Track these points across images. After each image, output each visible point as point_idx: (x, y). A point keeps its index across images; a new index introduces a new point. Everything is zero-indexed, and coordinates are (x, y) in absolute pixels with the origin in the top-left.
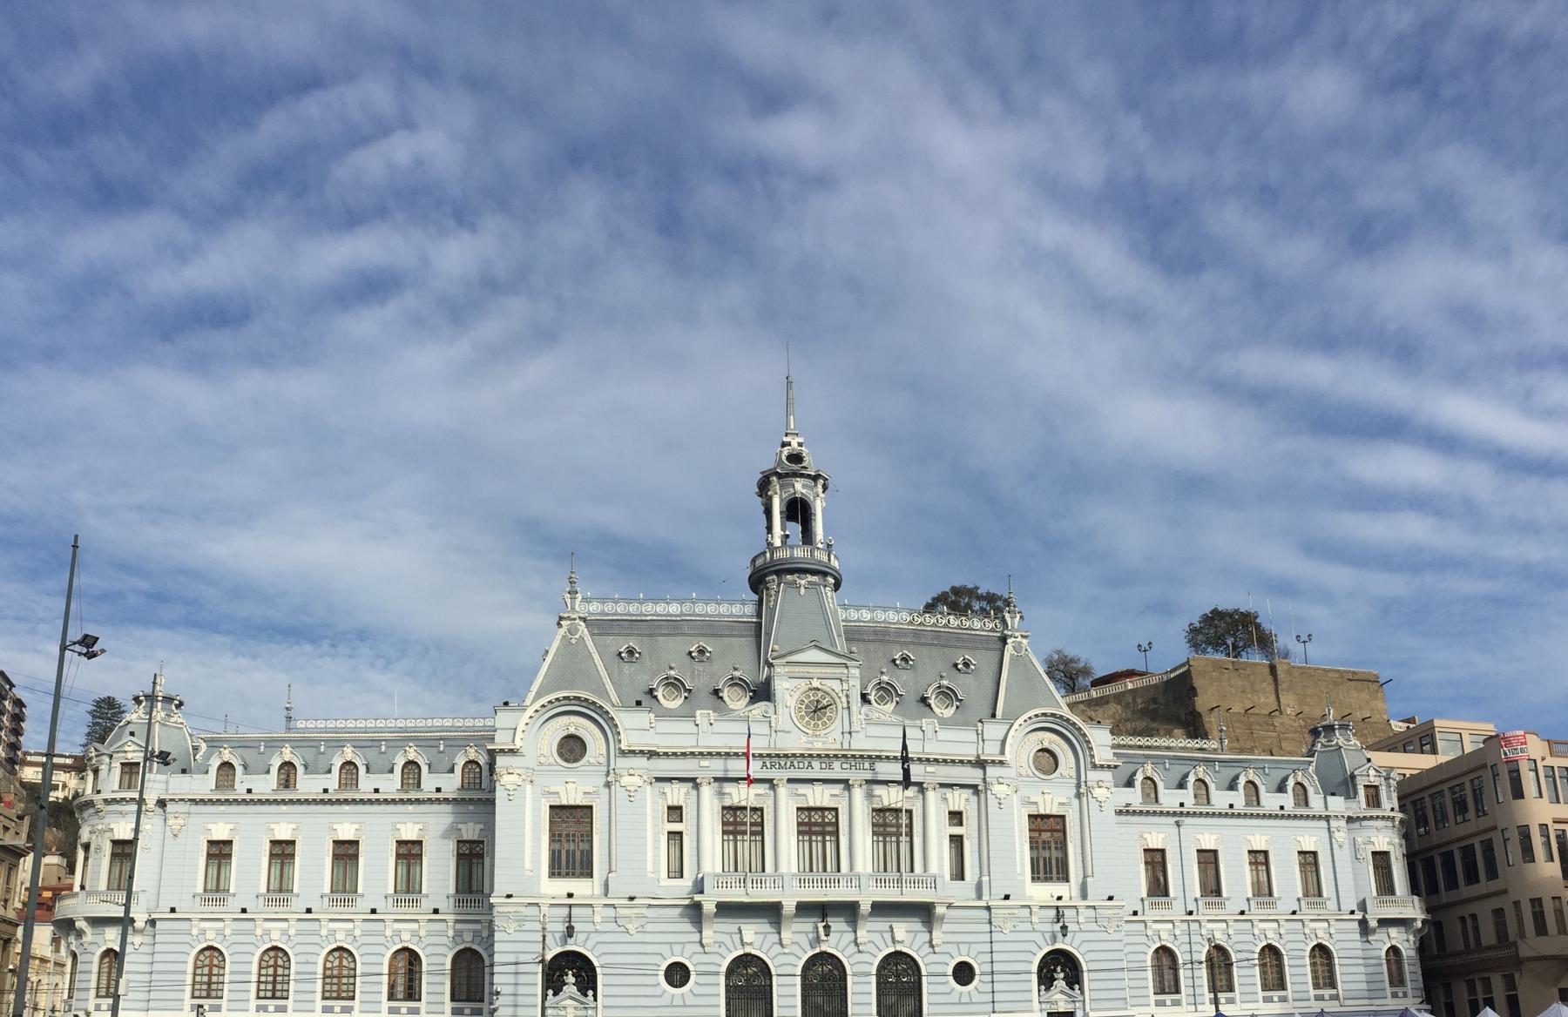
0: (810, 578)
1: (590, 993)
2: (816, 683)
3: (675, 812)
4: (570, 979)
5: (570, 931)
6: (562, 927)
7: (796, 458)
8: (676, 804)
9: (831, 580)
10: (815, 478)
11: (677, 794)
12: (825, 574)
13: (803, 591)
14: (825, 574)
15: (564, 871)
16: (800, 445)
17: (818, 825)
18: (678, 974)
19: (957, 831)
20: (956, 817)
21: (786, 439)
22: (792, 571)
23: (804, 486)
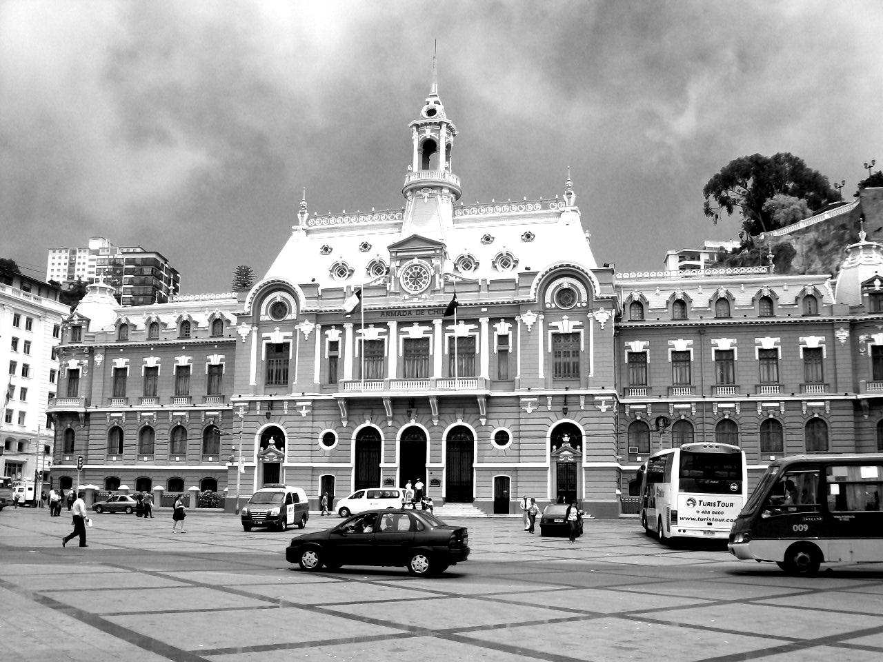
0: (431, 191)
1: (282, 449)
2: (416, 261)
3: (334, 345)
4: (272, 441)
5: (268, 416)
6: (264, 413)
7: (431, 112)
8: (333, 340)
9: (445, 191)
10: (440, 124)
11: (333, 335)
12: (442, 188)
13: (426, 200)
14: (442, 188)
15: (274, 381)
16: (437, 102)
17: (416, 351)
18: (329, 439)
19: (502, 348)
20: (503, 339)
21: (427, 100)
22: (420, 188)
23: (432, 131)
